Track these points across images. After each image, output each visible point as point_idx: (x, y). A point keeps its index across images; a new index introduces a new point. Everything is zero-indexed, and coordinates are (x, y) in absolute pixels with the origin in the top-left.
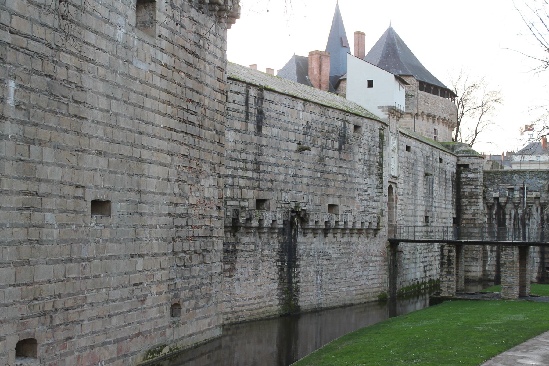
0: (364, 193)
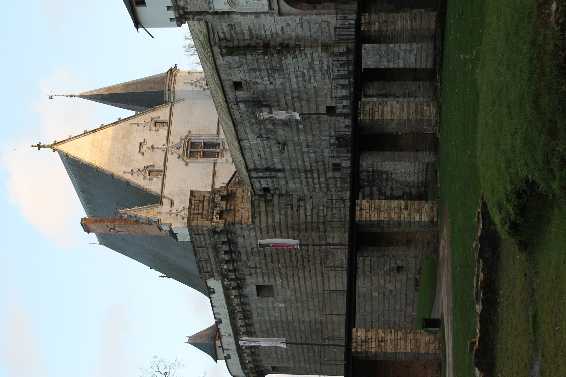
0: (307, 77)
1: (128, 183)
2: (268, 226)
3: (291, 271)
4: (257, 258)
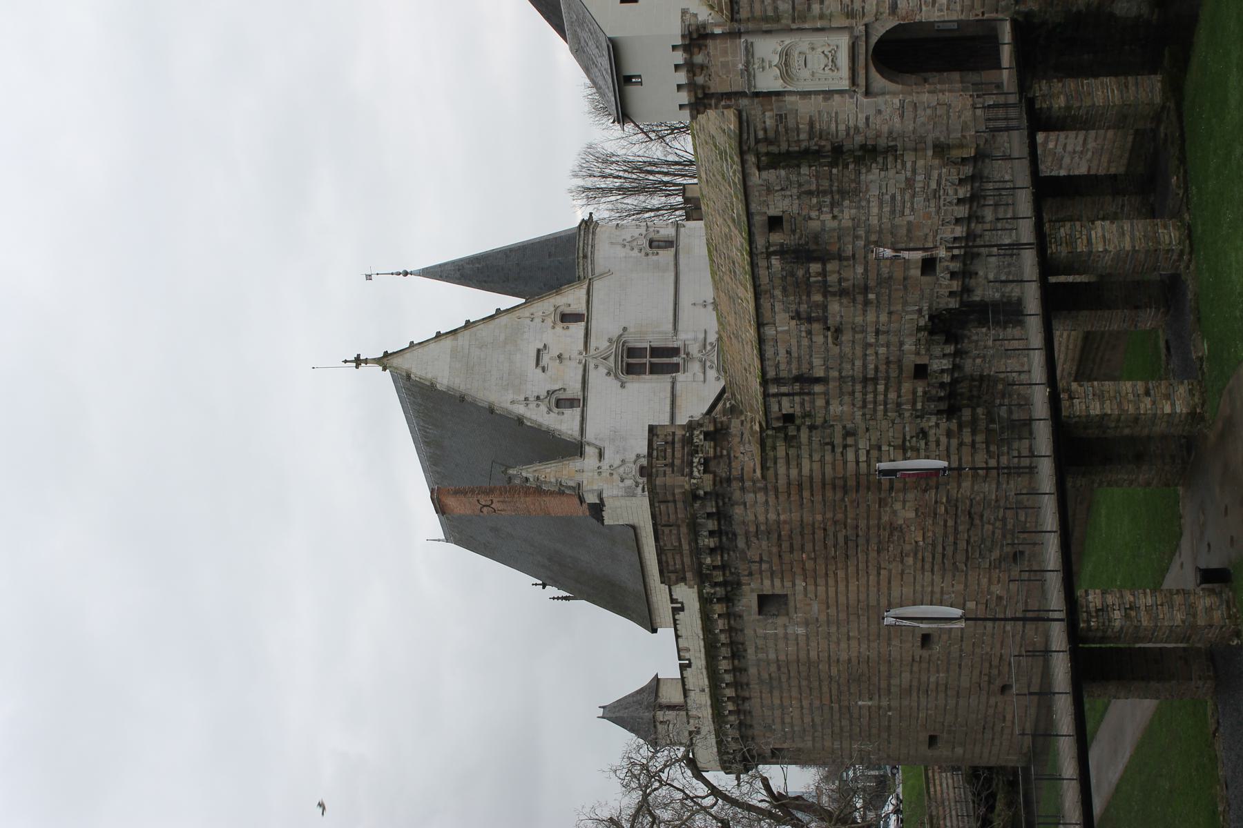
1: (520, 420)
2: (789, 484)
3: (823, 566)
4: (764, 543)
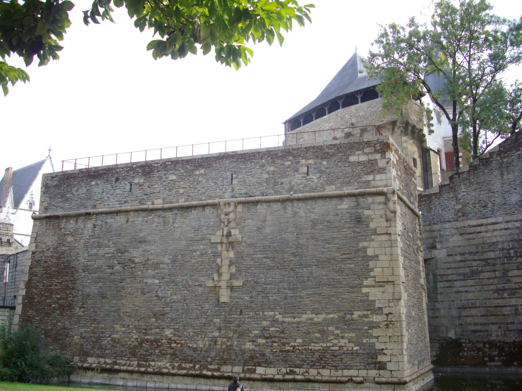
1: (26, 192)
